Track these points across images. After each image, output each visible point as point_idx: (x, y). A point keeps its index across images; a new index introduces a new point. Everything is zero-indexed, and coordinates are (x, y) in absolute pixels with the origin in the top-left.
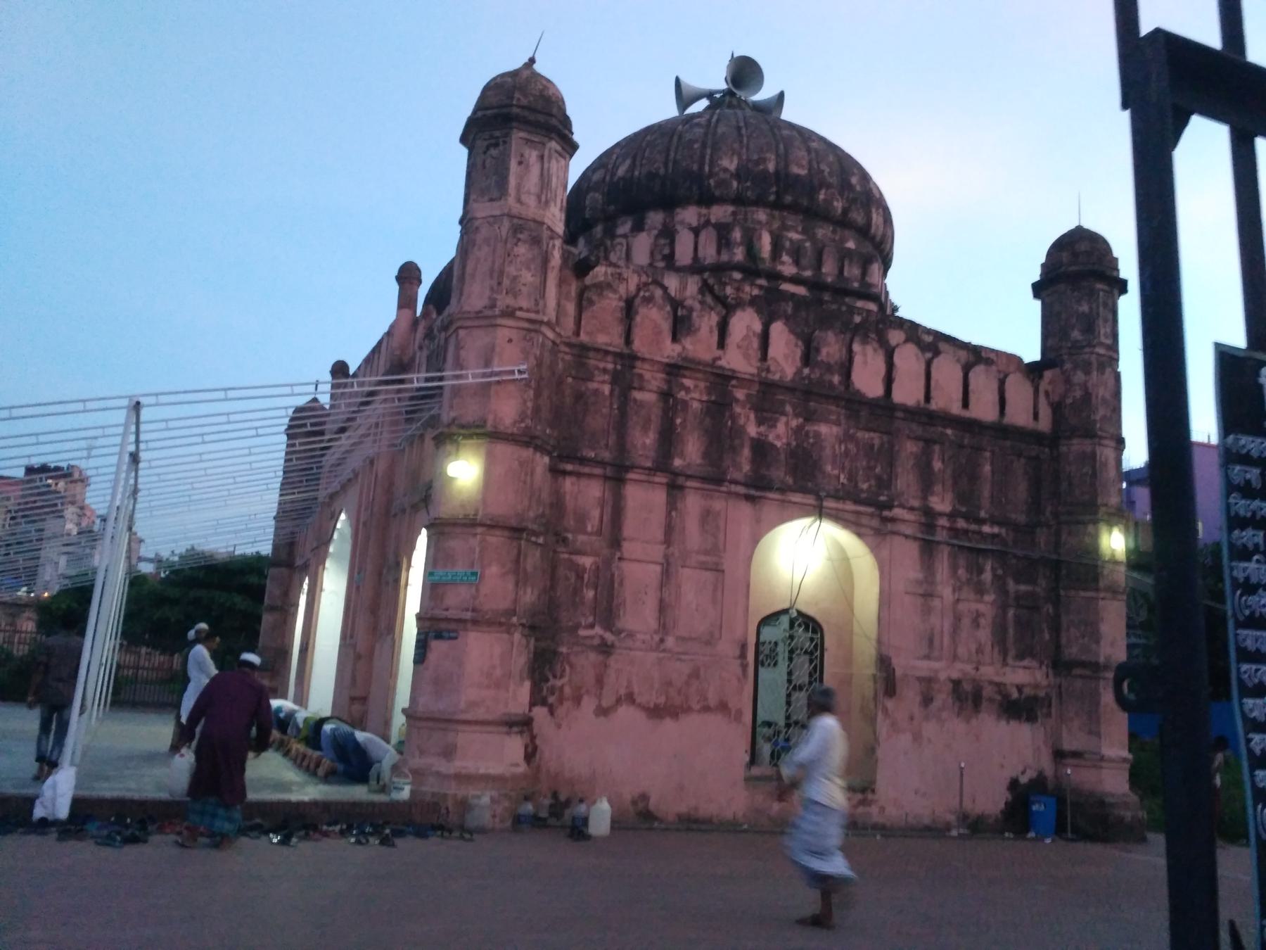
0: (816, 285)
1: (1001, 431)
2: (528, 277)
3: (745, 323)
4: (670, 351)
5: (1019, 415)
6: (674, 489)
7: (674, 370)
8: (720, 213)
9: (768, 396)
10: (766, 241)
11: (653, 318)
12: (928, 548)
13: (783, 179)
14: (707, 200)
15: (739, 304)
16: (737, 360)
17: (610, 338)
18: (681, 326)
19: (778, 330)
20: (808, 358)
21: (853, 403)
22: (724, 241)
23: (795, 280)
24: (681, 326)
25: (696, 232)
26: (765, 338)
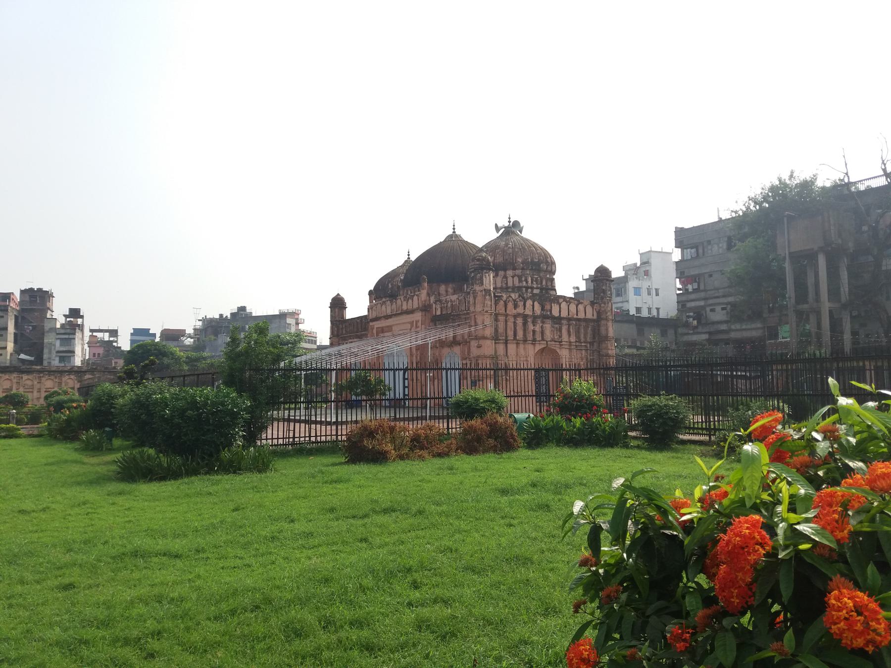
0: (541, 289)
1: (585, 320)
2: (489, 303)
3: (529, 303)
4: (514, 312)
5: (589, 316)
6: (518, 344)
7: (515, 317)
8: (518, 272)
9: (535, 318)
10: (529, 279)
11: (510, 305)
12: (570, 349)
13: (532, 262)
14: (514, 269)
15: (528, 299)
16: (528, 312)
17: (503, 311)
18: (516, 306)
19: (536, 303)
20: (543, 309)
21: (553, 318)
22: (520, 281)
23: (537, 288)
24: (516, 306)
25: (513, 277)
26: (533, 306)
